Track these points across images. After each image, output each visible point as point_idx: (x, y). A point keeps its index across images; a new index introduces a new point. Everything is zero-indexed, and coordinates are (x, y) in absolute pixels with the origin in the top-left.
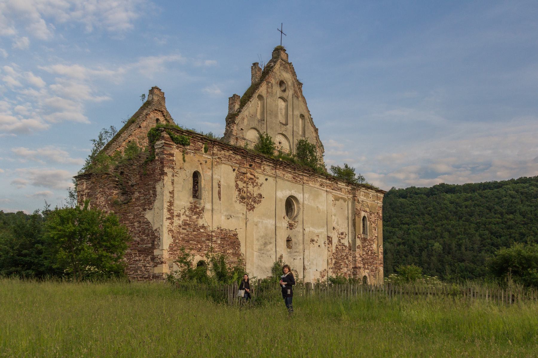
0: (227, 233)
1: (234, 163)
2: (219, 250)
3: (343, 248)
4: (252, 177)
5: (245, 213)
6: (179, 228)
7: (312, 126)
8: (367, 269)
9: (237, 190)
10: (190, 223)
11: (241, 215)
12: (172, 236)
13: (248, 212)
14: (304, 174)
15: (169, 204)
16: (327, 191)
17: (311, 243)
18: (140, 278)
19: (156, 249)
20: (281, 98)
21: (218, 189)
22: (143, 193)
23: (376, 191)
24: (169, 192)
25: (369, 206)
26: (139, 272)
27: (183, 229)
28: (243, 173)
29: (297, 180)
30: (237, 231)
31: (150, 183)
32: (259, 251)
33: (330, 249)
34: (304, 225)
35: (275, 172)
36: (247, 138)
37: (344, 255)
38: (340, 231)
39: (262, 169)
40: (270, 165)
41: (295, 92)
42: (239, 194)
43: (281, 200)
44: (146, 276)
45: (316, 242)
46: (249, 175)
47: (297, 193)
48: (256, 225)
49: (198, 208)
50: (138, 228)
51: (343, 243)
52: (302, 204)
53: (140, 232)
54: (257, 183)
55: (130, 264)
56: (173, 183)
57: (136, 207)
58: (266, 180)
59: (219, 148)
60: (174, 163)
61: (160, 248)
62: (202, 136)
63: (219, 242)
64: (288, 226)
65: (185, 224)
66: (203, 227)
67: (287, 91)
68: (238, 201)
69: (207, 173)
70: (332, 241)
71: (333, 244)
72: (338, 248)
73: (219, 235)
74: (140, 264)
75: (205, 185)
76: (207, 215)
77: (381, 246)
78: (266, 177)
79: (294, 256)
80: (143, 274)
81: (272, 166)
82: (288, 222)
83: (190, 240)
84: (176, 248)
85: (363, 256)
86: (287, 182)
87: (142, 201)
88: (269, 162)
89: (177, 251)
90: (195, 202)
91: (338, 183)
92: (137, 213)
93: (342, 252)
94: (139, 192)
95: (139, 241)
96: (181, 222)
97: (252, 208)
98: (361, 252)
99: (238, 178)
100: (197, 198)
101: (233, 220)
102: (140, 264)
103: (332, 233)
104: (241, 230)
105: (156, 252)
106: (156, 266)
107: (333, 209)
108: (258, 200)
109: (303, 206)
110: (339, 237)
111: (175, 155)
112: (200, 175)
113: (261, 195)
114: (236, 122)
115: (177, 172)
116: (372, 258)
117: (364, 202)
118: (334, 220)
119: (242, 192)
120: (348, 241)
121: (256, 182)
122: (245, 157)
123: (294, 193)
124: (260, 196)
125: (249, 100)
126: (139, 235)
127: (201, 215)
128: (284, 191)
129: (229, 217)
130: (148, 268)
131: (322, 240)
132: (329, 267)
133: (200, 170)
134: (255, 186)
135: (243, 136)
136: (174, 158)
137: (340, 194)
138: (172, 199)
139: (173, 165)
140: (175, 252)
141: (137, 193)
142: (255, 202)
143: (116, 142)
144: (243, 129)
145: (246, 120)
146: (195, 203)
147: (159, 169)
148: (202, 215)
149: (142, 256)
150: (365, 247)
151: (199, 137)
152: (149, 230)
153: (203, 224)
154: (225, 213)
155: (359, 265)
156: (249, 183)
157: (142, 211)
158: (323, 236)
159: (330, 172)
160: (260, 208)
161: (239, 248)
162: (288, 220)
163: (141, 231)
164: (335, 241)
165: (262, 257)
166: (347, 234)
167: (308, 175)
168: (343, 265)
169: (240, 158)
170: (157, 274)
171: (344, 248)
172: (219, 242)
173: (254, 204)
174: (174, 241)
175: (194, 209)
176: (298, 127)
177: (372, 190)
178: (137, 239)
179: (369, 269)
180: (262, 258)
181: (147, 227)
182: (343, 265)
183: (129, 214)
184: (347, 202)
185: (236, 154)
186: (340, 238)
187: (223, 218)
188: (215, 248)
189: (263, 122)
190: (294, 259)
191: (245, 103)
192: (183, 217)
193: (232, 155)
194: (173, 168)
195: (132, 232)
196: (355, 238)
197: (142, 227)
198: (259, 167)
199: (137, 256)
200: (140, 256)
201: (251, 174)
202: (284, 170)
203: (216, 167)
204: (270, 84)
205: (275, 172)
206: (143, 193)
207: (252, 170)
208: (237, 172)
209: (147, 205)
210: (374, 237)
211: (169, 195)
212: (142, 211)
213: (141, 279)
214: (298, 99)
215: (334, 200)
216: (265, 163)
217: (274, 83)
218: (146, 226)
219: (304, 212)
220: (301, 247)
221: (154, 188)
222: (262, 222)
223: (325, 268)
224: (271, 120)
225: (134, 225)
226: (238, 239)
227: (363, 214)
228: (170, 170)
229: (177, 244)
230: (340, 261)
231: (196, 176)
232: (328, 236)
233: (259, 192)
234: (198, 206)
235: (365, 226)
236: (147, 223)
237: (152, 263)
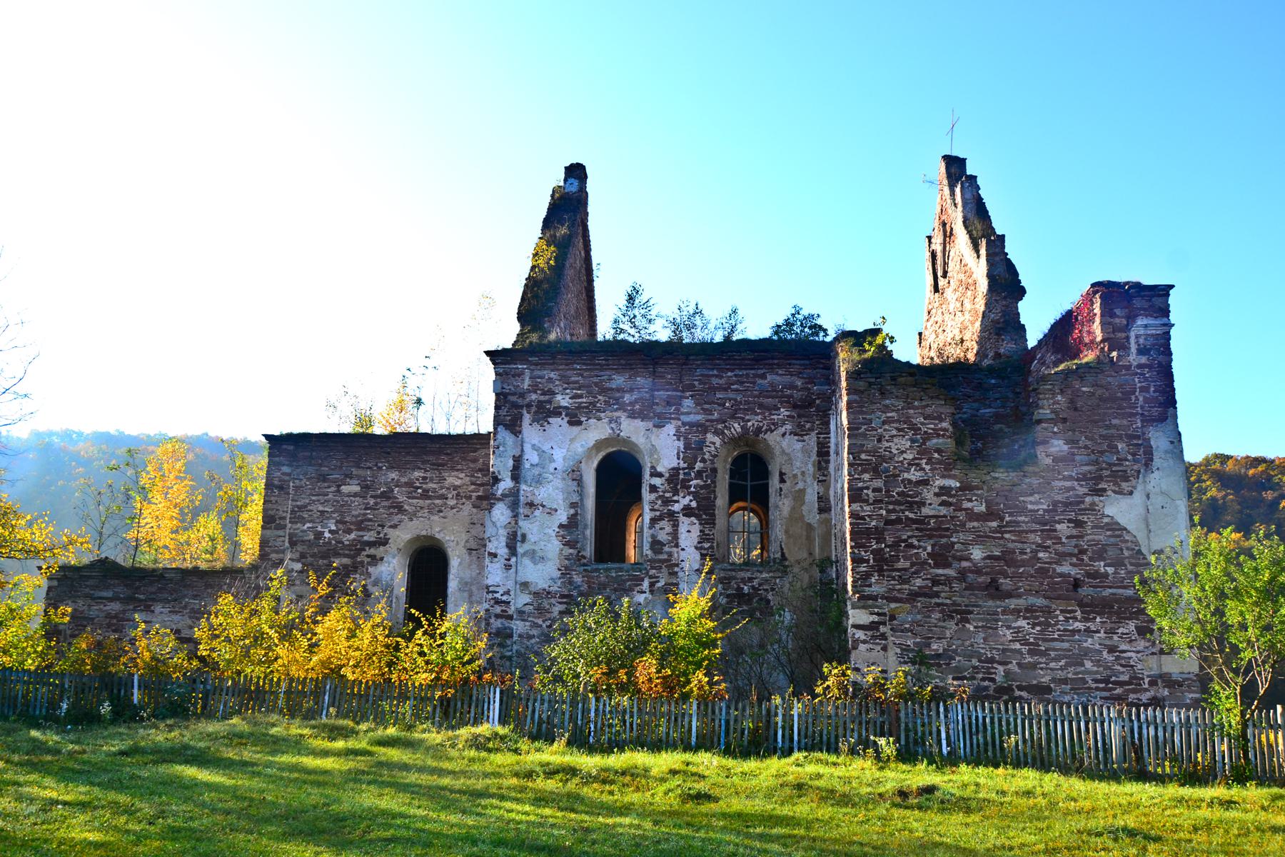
18: (1096, 681)
22: (1086, 447)
26: (1088, 664)
31: (1115, 422)
44: (1125, 678)
50: (1074, 542)
53: (1083, 552)
55: (1045, 640)
74: (1088, 643)
80: (1109, 672)
95: (1079, 576)
102: (1088, 643)
130: (1129, 654)
141: (1061, 442)
147: (1154, 392)
149: (1098, 619)
163: (1087, 550)
178: (1065, 568)
181: (1112, 540)
197: (1094, 540)
199: (1075, 619)
200: (1086, 620)
206: (1086, 447)
213: (1103, 685)
225: (1055, 530)
237: (1141, 644)
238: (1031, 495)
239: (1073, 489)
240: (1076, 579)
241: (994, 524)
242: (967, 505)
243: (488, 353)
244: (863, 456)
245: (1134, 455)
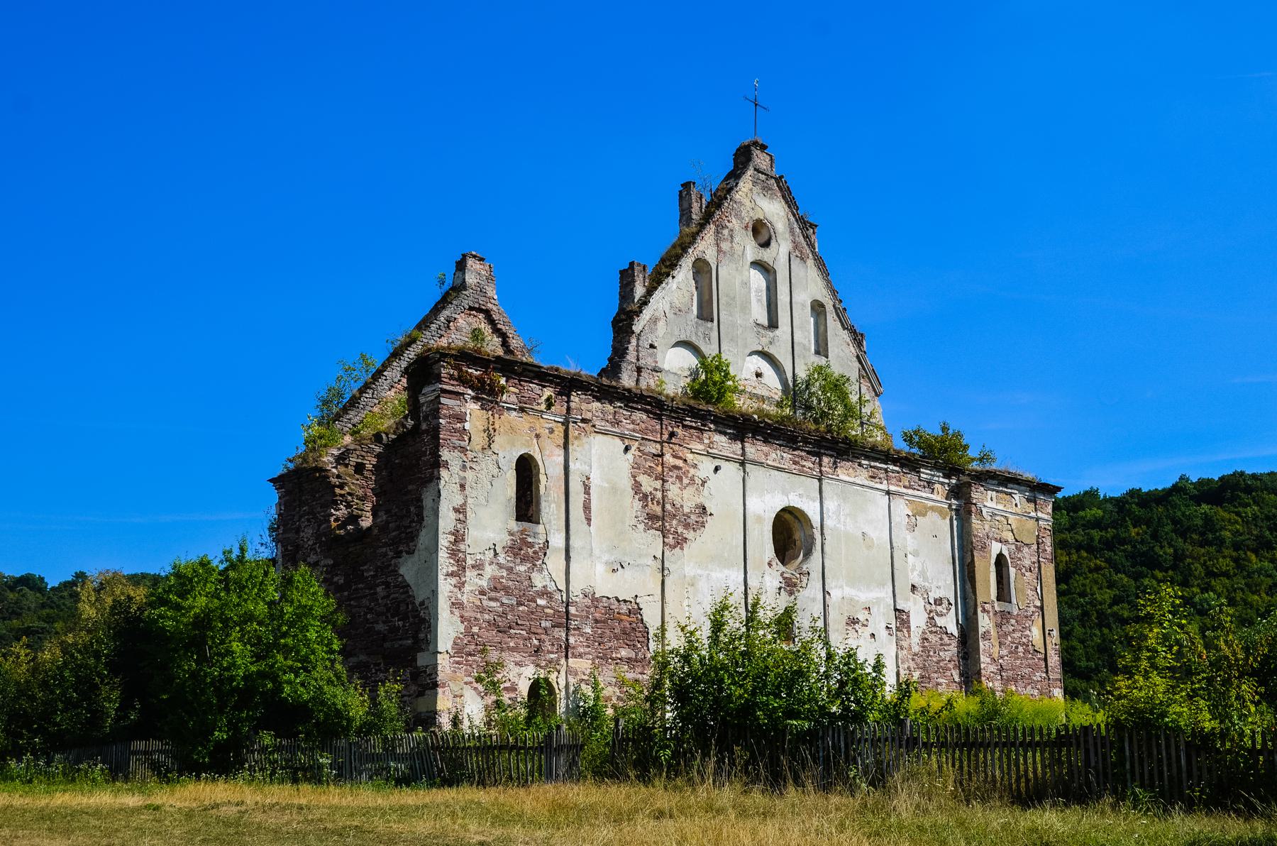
0: (612, 607)
1: (628, 429)
2: (587, 650)
3: (941, 639)
4: (680, 463)
5: (659, 556)
6: (481, 597)
9: (637, 497)
10: (510, 583)
11: (650, 561)
12: (462, 617)
13: (667, 553)
14: (822, 451)
15: (452, 538)
16: (888, 493)
17: (850, 628)
19: (423, 650)
20: (757, 264)
21: (582, 497)
23: (1029, 486)
24: (454, 509)
25: (1013, 527)
27: (490, 599)
28: (654, 455)
29: (804, 466)
31: (410, 487)
33: (905, 644)
34: (827, 581)
35: (743, 448)
36: (666, 366)
37: (948, 659)
38: (933, 596)
39: (706, 441)
41: (796, 246)
42: (643, 507)
43: (759, 519)
45: (864, 625)
46: (668, 458)
47: (804, 499)
48: (693, 585)
49: (531, 545)
51: (941, 627)
52: (819, 528)
54: (692, 479)
56: (462, 486)
57: (381, 547)
58: (717, 469)
59: (586, 395)
60: (466, 438)
61: (431, 647)
62: (537, 369)
63: (588, 630)
64: (783, 586)
65: (496, 587)
66: (544, 593)
67: (773, 243)
68: (641, 527)
69: (555, 458)
70: (909, 622)
71: (912, 629)
72: (926, 639)
73: (588, 612)
76: (555, 563)
77: (1056, 633)
78: (717, 462)
81: (733, 434)
82: (782, 575)
83: (510, 628)
84: (473, 647)
85: (1001, 661)
86: (776, 472)
87: (394, 534)
88: (725, 425)
89: (474, 655)
90: (522, 532)
92: (383, 563)
93: (940, 650)
94: (387, 512)
95: (386, 632)
97: (680, 542)
98: (995, 651)
99: (639, 469)
100: (530, 521)
101: (627, 574)
103: (907, 599)
104: (650, 598)
105: (422, 659)
106: (421, 694)
107: (909, 537)
108: (697, 522)
109: (822, 534)
110: (931, 611)
111: (468, 419)
112: (537, 465)
113: (704, 509)
114: (634, 328)
115: (475, 460)
116: (1029, 666)
117: (997, 518)
118: (914, 566)
119: (650, 503)
120: (955, 622)
121: (690, 475)
123: (797, 499)
124: (703, 510)
125: (668, 275)
126: (387, 617)
127: (537, 563)
128: (769, 496)
129: (617, 567)
131: (881, 619)
133: (534, 452)
135: (657, 362)
136: (467, 426)
137: (927, 499)
138: (459, 526)
139: (462, 444)
140: (470, 658)
142: (687, 526)
143: (371, 391)
145: (661, 324)
146: (522, 534)
148: (540, 562)
150: (1006, 635)
151: (530, 371)
152: (408, 605)
154: (606, 557)
156: (670, 480)
157: (393, 558)
158: (882, 610)
159: (900, 445)
160: (700, 543)
162: (783, 569)
164: (918, 620)
166: (953, 601)
169: (645, 417)
170: (423, 715)
171: (946, 639)
172: (588, 630)
173: (684, 531)
174: (468, 632)
175: (520, 549)
176: (807, 333)
178: (380, 627)
181: (403, 596)
183: (365, 567)
184: (948, 521)
185: (632, 408)
186: (932, 615)
187: (600, 569)
189: (709, 324)
191: (660, 283)
192: (489, 571)
193: (621, 411)
194: (463, 450)
195: (372, 609)
196: (975, 613)
197: (393, 599)
199: (380, 670)
201: (675, 457)
202: (766, 441)
203: (576, 442)
204: (726, 232)
205: (743, 448)
207: (676, 447)
208: (637, 453)
209: (404, 543)
210: (1033, 609)
211: (453, 515)
212: (393, 558)
214: (805, 262)
215: (910, 514)
216: (712, 426)
217: (737, 227)
218: (402, 594)
219: (827, 548)
221: (420, 500)
224: (730, 318)
225: (376, 593)
227: (996, 548)
228: (457, 454)
229: (476, 637)
230: (936, 675)
231: (526, 469)
232: (896, 610)
233: (699, 501)
234: (530, 540)
235: (1005, 581)
236: (403, 587)
238: (365, 564)
239: (385, 555)
240: (384, 635)
241: (346, 593)
242: (336, 579)
243: (271, 481)
244: (289, 548)
245: (418, 515)
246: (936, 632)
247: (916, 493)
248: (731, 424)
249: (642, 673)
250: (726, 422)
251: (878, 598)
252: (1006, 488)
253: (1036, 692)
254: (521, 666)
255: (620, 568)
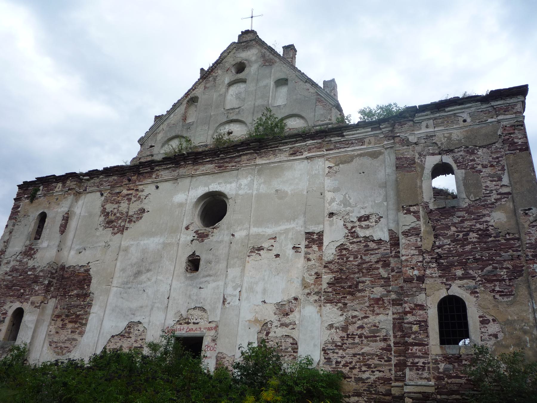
7: (306, 82)
8: (461, 278)
9: (102, 215)
17: (254, 254)
30: (90, 264)
32: (123, 286)
40: (168, 167)
54: (139, 197)
58: (157, 187)
75: (48, 223)
79: (201, 283)
81: (173, 167)
86: (201, 177)
88: (166, 164)
91: (344, 134)
96: (8, 270)
97: (122, 230)
122: (123, 174)
123: (215, 186)
124: (143, 211)
132: (307, 291)
134: (135, 201)
144: (153, 145)
153: (34, 266)
155: (416, 272)
161: (89, 286)
165: (126, 293)
167: (252, 151)
168: (368, 282)
169: (116, 178)
171: (372, 245)
177: (460, 104)
179: (473, 278)
180: (125, 295)
182: (368, 282)
188: (40, 290)
190: (200, 288)
192: (12, 264)
198: (149, 176)
201: (128, 190)
215: (332, 165)
216: (157, 168)
220: (223, 265)
222: (137, 245)
223: (293, 295)
226: (89, 274)
233: (140, 207)
246: (360, 242)
247: (342, 150)
248: (168, 162)
249: (83, 301)
250: (165, 163)
251: (286, 229)
252: (445, 112)
253: (503, 273)
254: (12, 303)
255: (83, 251)
